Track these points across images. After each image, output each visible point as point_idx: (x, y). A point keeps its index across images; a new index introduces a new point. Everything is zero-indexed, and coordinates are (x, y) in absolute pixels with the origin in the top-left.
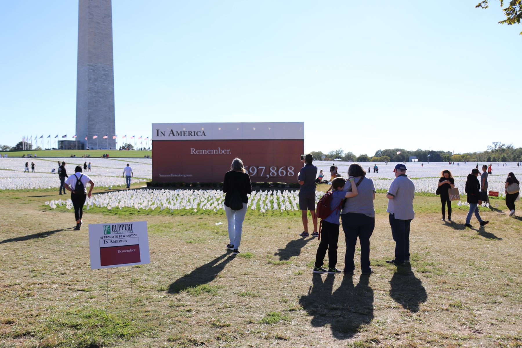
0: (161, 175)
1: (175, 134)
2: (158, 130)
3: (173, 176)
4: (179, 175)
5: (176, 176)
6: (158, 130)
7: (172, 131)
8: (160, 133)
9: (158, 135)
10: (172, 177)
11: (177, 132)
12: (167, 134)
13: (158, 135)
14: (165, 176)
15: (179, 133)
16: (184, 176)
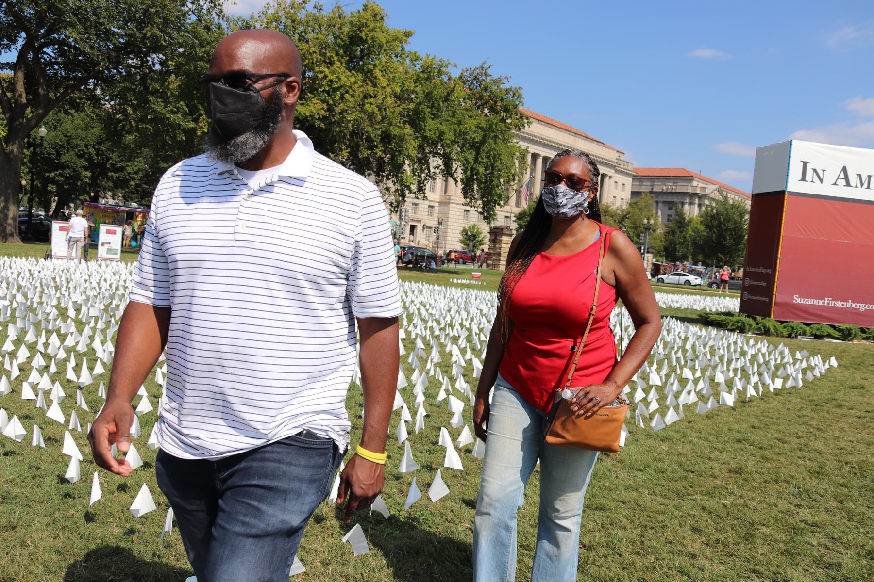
0: (797, 300)
1: (853, 179)
2: (805, 164)
3: (832, 304)
4: (849, 305)
5: (839, 304)
6: (805, 164)
7: (844, 169)
8: (809, 172)
9: (803, 179)
10: (828, 307)
11: (860, 176)
12: (829, 178)
13: (803, 179)
14: (810, 302)
15: (864, 178)
16: (862, 307)
